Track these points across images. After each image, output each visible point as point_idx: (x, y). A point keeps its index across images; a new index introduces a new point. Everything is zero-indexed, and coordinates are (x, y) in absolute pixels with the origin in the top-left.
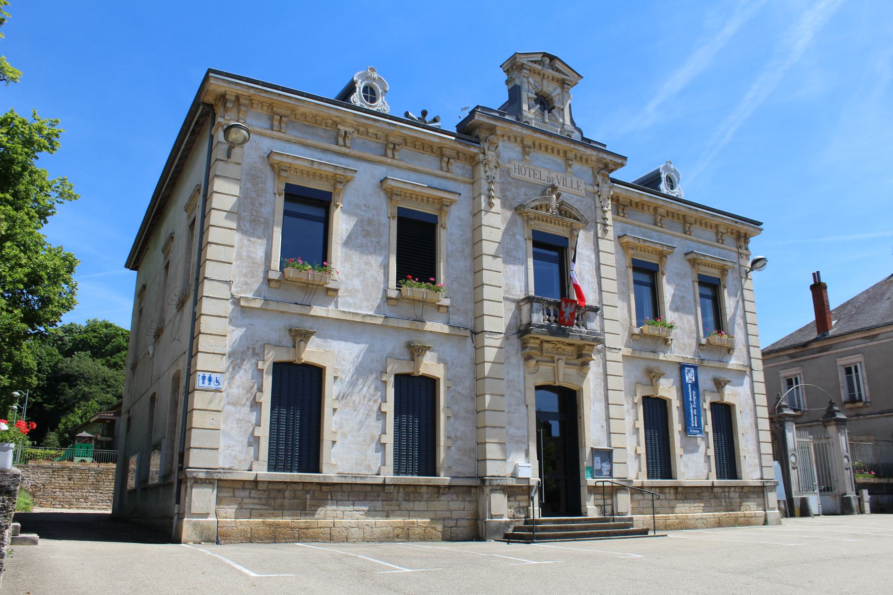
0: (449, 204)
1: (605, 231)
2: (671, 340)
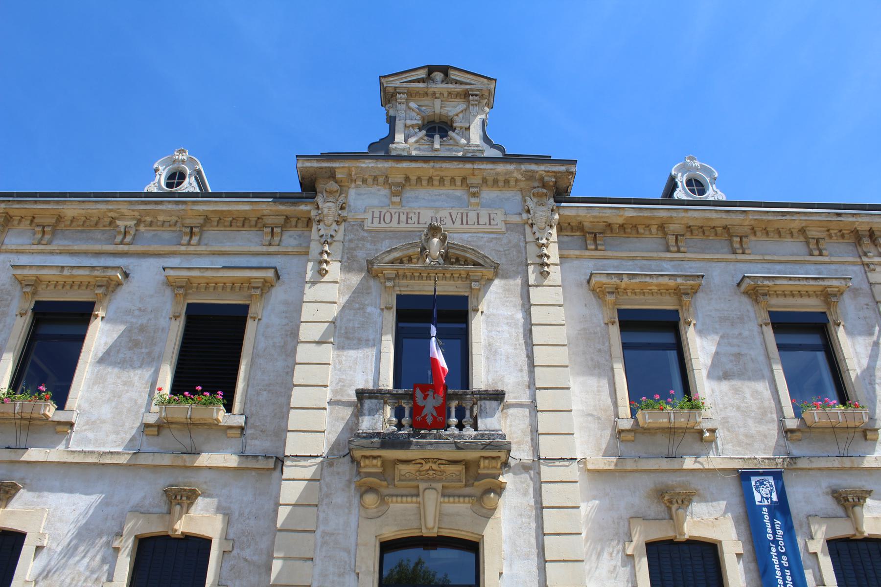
0: (260, 285)
1: (544, 275)
2: (713, 431)
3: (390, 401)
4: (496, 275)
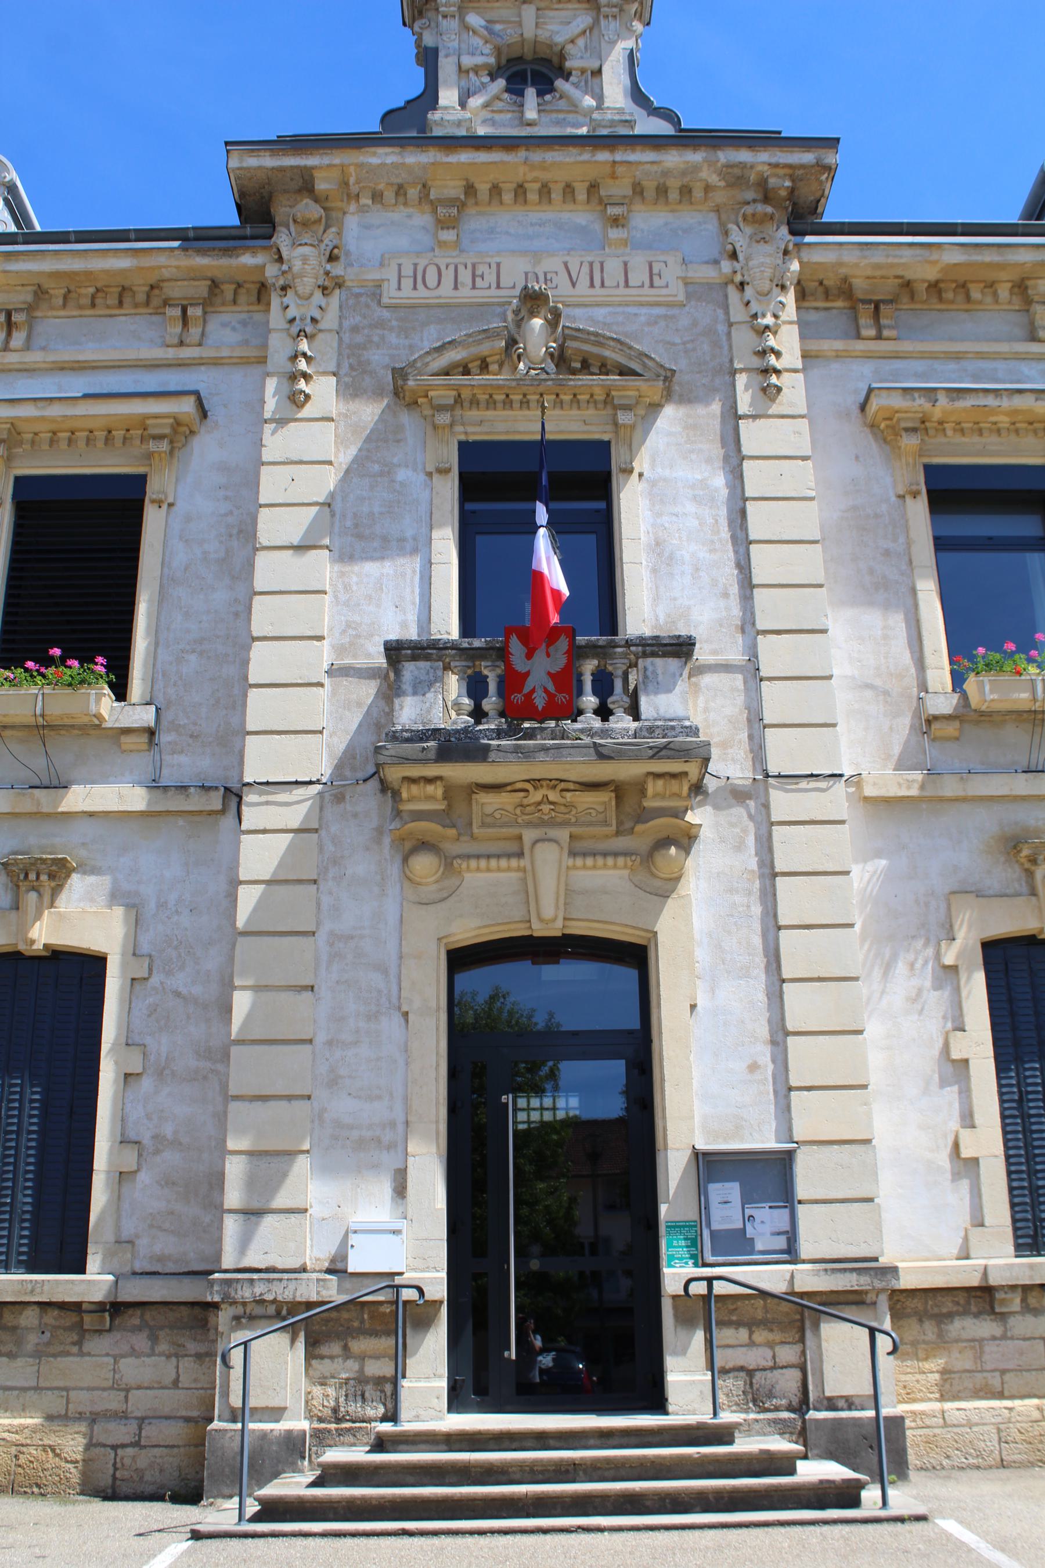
1: (770, 393)
3: (457, 664)
4: (668, 395)
